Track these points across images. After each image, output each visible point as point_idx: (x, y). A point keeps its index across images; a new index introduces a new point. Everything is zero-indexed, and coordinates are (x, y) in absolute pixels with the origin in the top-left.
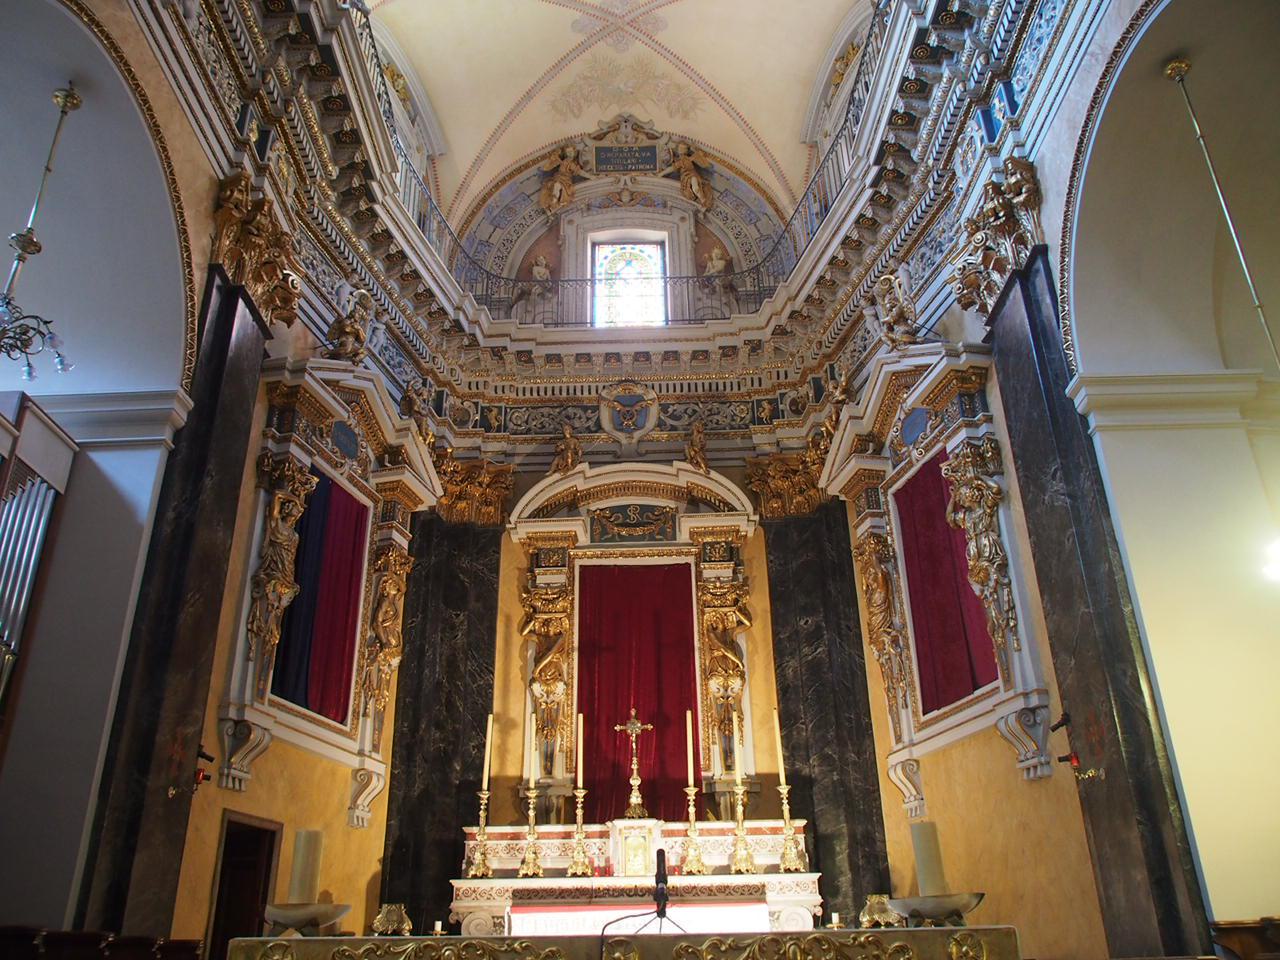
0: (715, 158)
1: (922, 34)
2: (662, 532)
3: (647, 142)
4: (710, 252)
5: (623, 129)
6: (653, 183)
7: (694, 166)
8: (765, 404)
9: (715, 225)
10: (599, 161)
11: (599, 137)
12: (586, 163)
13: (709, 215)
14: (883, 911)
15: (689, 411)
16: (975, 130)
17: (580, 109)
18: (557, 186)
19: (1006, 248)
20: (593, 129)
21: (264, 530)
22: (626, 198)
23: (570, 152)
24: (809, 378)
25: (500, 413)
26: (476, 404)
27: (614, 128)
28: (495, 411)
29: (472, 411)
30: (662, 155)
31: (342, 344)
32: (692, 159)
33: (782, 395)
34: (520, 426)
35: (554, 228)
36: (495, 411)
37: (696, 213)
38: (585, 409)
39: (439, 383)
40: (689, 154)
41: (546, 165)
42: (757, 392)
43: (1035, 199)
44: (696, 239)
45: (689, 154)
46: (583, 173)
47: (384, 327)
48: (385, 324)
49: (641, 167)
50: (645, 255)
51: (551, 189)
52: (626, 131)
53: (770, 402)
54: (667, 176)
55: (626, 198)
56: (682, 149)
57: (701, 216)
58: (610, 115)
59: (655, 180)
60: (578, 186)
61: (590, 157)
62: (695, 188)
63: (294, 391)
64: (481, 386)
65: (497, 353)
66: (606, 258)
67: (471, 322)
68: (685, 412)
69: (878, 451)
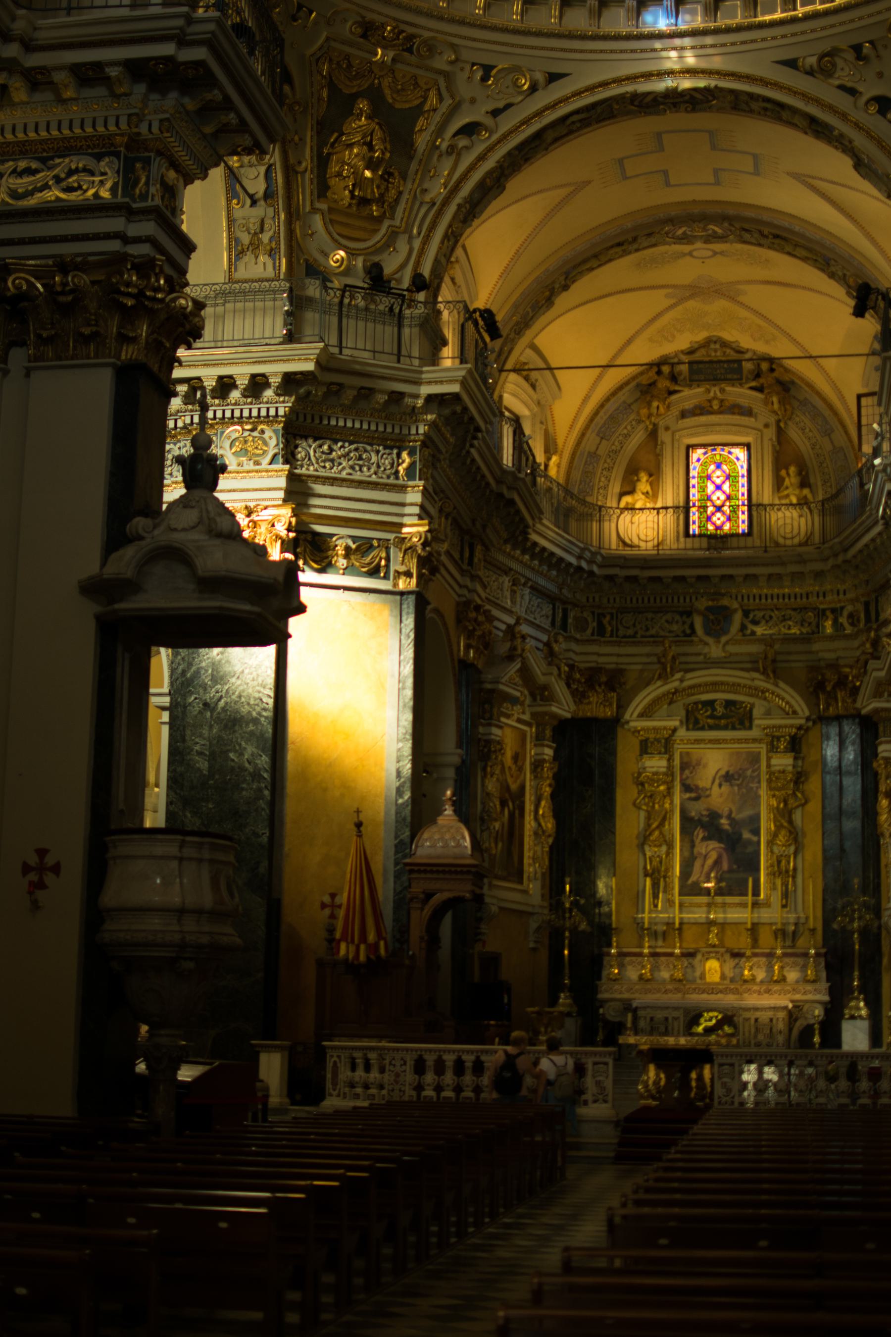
0: (794, 374)
2: (742, 723)
3: (734, 356)
4: (787, 469)
5: (712, 346)
7: (775, 381)
8: (828, 613)
9: (794, 433)
10: (691, 371)
11: (691, 352)
12: (680, 373)
13: (790, 423)
14: (859, 1009)
15: (767, 617)
17: (674, 337)
18: (655, 404)
21: (483, 785)
23: (666, 369)
24: (862, 600)
25: (612, 618)
26: (593, 613)
28: (608, 618)
29: (590, 619)
30: (748, 366)
32: (775, 374)
33: (842, 608)
34: (628, 628)
35: (653, 434)
36: (608, 618)
37: (779, 421)
38: (681, 614)
39: (564, 602)
40: (772, 370)
41: (644, 380)
42: (821, 603)
44: (778, 448)
45: (772, 370)
46: (677, 388)
47: (527, 591)
48: (532, 588)
49: (729, 376)
50: (733, 457)
51: (649, 405)
52: (718, 346)
53: (833, 611)
54: (751, 388)
55: (716, 405)
56: (765, 366)
57: (782, 425)
58: (701, 336)
59: (741, 390)
60: (674, 397)
61: (684, 368)
62: (776, 406)
63: (492, 691)
64: (597, 599)
65: (610, 578)
66: (698, 460)
67: (590, 562)
68: (763, 617)
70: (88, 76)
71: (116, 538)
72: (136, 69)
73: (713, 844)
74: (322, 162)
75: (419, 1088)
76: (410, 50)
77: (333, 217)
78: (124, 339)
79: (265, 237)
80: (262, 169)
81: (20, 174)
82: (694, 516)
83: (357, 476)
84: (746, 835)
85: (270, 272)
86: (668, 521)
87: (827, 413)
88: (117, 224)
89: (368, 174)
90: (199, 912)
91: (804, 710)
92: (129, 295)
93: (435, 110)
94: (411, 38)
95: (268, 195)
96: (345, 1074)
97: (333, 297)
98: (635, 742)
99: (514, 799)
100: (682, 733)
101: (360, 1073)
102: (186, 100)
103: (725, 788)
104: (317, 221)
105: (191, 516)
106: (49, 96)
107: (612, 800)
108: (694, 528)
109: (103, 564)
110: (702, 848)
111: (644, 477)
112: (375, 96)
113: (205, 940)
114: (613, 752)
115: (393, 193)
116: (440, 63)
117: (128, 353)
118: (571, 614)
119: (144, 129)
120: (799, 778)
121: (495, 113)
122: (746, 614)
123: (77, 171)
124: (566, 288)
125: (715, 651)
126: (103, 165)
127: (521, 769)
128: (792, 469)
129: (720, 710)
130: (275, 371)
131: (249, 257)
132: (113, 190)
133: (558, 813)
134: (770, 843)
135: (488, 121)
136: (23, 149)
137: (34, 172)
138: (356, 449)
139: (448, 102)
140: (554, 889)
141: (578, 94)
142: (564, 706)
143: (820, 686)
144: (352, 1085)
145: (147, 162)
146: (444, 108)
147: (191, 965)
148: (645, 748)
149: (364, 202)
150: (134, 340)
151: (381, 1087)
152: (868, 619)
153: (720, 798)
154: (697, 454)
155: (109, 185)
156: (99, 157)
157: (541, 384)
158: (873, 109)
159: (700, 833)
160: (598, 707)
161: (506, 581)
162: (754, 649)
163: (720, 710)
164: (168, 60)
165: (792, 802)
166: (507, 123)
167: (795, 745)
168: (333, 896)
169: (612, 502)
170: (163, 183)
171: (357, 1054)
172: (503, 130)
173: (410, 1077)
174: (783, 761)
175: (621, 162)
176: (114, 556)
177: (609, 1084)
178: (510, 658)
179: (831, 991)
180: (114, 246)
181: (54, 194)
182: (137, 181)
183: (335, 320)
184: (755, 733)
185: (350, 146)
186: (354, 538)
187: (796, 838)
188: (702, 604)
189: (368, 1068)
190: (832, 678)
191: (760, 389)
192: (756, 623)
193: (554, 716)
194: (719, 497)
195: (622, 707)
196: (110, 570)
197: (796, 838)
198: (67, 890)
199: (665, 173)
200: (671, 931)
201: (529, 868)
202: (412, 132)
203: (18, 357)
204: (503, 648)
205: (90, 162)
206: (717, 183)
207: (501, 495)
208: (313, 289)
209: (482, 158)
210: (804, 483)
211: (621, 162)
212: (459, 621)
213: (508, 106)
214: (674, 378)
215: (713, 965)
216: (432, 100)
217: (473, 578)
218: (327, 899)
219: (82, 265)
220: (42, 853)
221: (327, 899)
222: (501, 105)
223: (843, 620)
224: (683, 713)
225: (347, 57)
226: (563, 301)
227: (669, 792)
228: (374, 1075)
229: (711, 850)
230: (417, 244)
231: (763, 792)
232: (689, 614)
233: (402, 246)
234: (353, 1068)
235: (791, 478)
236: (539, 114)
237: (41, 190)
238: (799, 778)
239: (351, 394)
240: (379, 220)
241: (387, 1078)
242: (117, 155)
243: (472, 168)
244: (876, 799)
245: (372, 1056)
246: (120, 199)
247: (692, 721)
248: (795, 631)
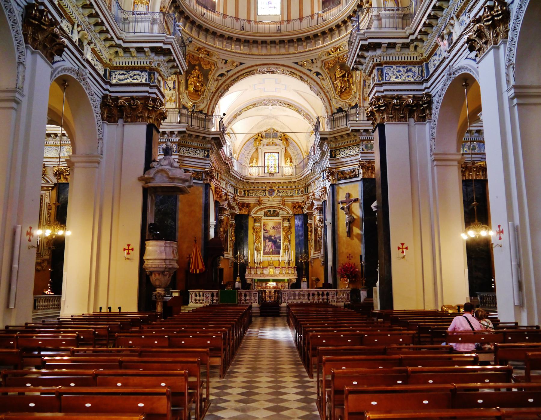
1: (314, 164)
6: (277, 141)
7: (285, 138)
9: (289, 150)
10: (266, 136)
16: (322, 174)
19: (323, 196)
20: (265, 130)
22: (271, 143)
23: (260, 135)
27: (270, 129)
30: (279, 134)
31: (226, 198)
35: (257, 150)
43: (326, 193)
55: (271, 143)
56: (283, 135)
58: (268, 128)
61: (264, 135)
65: (247, 182)
69: (312, 209)
70: (140, 50)
71: (148, 166)
72: (152, 49)
73: (270, 243)
74: (187, 81)
75: (212, 300)
76: (208, 55)
77: (190, 94)
78: (149, 117)
79: (173, 98)
81: (121, 75)
82: (266, 168)
83: (195, 156)
84: (278, 241)
85: (174, 107)
86: (261, 170)
87: (296, 145)
88: (147, 89)
89: (198, 84)
90: (170, 260)
91: (291, 213)
92: (150, 107)
94: (208, 52)
95: (174, 88)
96: (194, 298)
97: (189, 114)
98: (253, 220)
99: (226, 232)
100: (263, 218)
101: (198, 298)
102: (165, 58)
103: (273, 230)
104: (185, 95)
105: (166, 162)
106: (128, 55)
107: (248, 233)
108: (266, 172)
109: (144, 174)
110: (268, 243)
111: (255, 159)
112: (200, 66)
113: (171, 266)
114: (248, 222)
115: (203, 89)
116: (214, 59)
117: (150, 121)
118: (238, 190)
119: (153, 65)
120: (290, 228)
121: (228, 71)
122: (278, 191)
123: (136, 75)
124: (240, 115)
125: (271, 199)
126: (143, 74)
127: (228, 226)
128: (289, 158)
129: (272, 212)
130: (176, 130)
131: (169, 103)
132: (146, 80)
133: (236, 236)
134: (284, 242)
135: (226, 73)
136: (122, 68)
137: (124, 74)
139: (217, 68)
140: (235, 253)
141: (247, 68)
142: (237, 212)
143: (294, 207)
144: (196, 300)
145: (154, 74)
146: (215, 69)
147: (167, 273)
148: (255, 221)
149: (197, 91)
150: (151, 118)
151: (203, 300)
152: (305, 192)
153: (272, 232)
154: (266, 154)
155: (144, 79)
156: (142, 72)
157: (232, 137)
158: (315, 74)
159: (267, 240)
160: (244, 212)
161: (224, 182)
162: (279, 199)
163: (272, 212)
164: (161, 47)
165: (288, 233)
166: (230, 74)
167: (289, 221)
168: (189, 255)
169: (247, 165)
170: (158, 80)
171: (197, 293)
172: (229, 76)
173: (210, 298)
174: (286, 224)
175: (255, 85)
176: (147, 172)
177: (257, 298)
178: (226, 200)
179: (298, 276)
180: (147, 94)
181: (130, 80)
182: (151, 78)
183: (190, 119)
184: (280, 218)
185: (193, 77)
186: (194, 171)
187: (289, 241)
188: (268, 188)
189: (200, 296)
190: (297, 205)
191: (281, 140)
192: (280, 193)
193: (235, 213)
194: (271, 164)
195: (250, 212)
196: (146, 176)
197: (289, 241)
198: (136, 254)
200: (261, 263)
201: (229, 249)
202: (208, 75)
203: (121, 121)
204: (224, 198)
205: (140, 73)
206: (276, 91)
207: (225, 162)
208: (185, 111)
209: (224, 82)
210: (291, 162)
211: (255, 85)
212: (215, 191)
213: (231, 70)
214: (262, 137)
215: (271, 270)
216: (213, 67)
217: (218, 181)
218: (188, 256)
219: (138, 98)
220: (129, 246)
221: (188, 256)
223: (300, 192)
224: (263, 213)
225: (193, 56)
226: (239, 117)
227: (260, 231)
228: (201, 298)
229: (270, 244)
230: (209, 102)
231: (282, 231)
232: (265, 191)
233: (205, 101)
234: (196, 296)
235: (289, 160)
236: (238, 72)
237: (126, 79)
238: (290, 228)
239: (194, 136)
240: (200, 96)
241: (204, 298)
242: (147, 71)
243: (222, 84)
244: (308, 233)
245: (201, 293)
246: (147, 83)
247: (266, 215)
248: (289, 194)
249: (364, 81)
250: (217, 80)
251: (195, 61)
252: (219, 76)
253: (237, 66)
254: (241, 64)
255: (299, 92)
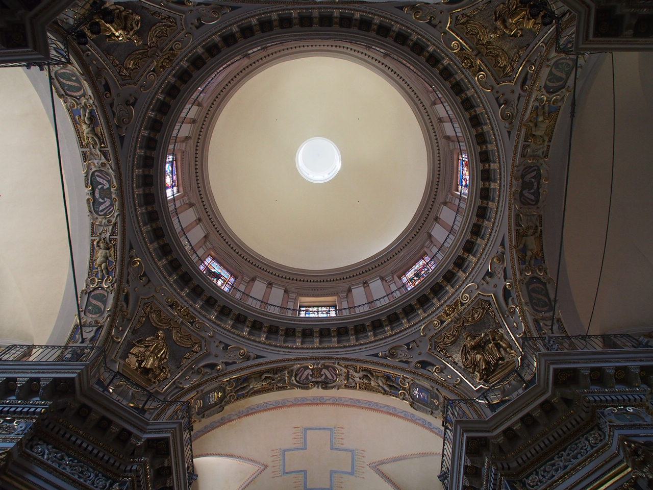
76: (192, 323)
80: (95, 329)
93: (197, 353)
112: (168, 333)
121: (227, 364)
138: (82, 467)
166: (230, 368)
199: (305, 472)
222: (230, 361)
225: (160, 311)
249: (536, 321)
250: (199, 372)
251: (160, 321)
252: (204, 366)
253: (248, 358)
254: (258, 357)
255: (384, 468)
